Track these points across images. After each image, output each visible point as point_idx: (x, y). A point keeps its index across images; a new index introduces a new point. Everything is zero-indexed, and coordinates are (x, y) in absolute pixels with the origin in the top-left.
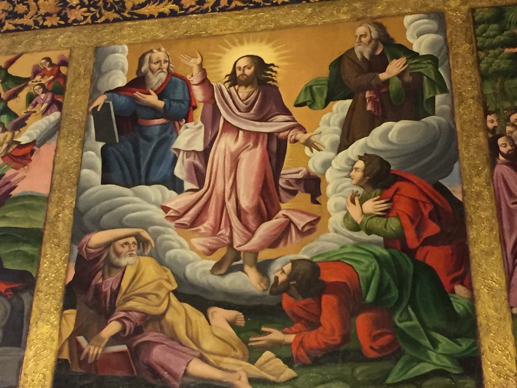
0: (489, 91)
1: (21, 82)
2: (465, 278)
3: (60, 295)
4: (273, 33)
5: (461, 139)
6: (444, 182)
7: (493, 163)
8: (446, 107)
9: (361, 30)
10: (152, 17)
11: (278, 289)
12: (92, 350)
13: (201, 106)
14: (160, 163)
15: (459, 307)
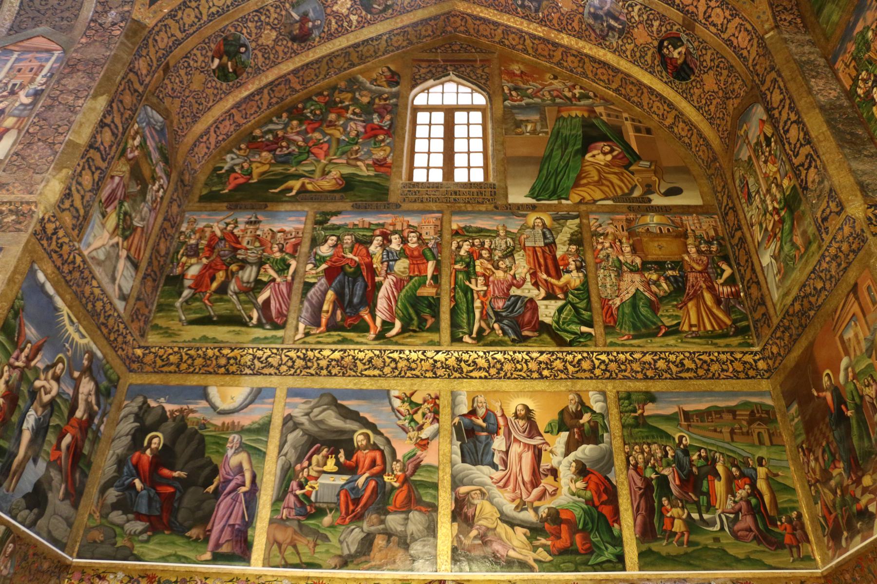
0: (625, 434)
1: (418, 406)
2: (618, 521)
3: (450, 516)
4: (533, 394)
5: (615, 456)
6: (609, 476)
7: (628, 469)
8: (608, 440)
9: (571, 396)
10: (476, 378)
11: (543, 520)
12: (467, 542)
13: (503, 428)
14: (487, 454)
15: (616, 533)
